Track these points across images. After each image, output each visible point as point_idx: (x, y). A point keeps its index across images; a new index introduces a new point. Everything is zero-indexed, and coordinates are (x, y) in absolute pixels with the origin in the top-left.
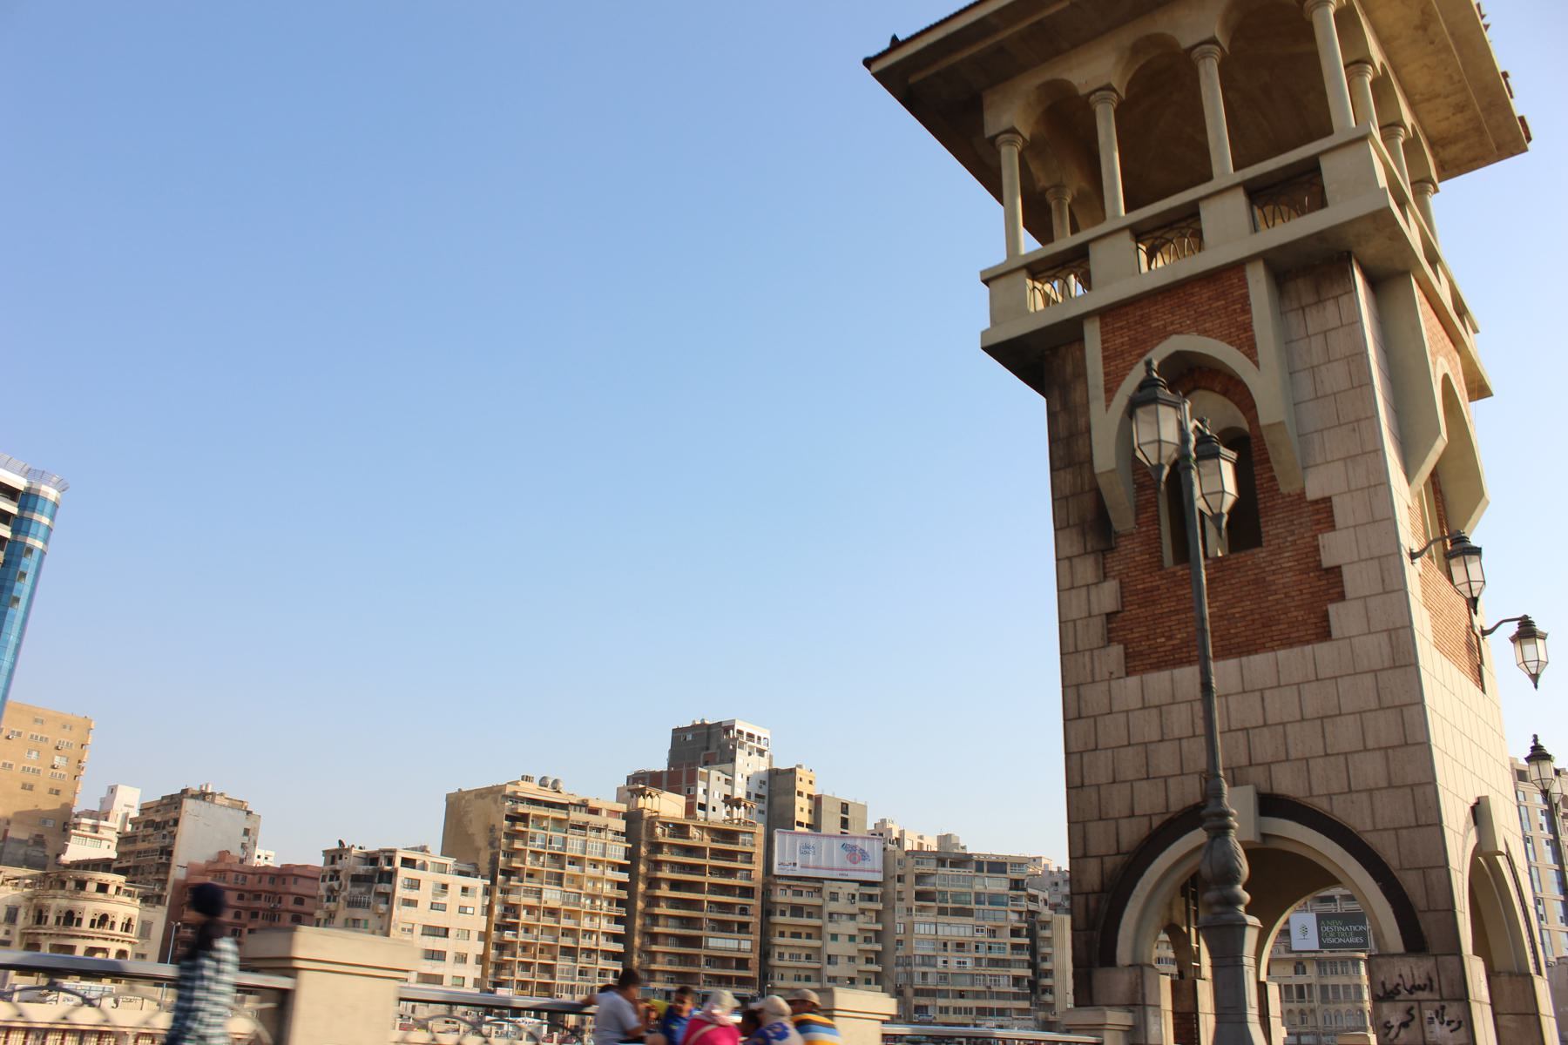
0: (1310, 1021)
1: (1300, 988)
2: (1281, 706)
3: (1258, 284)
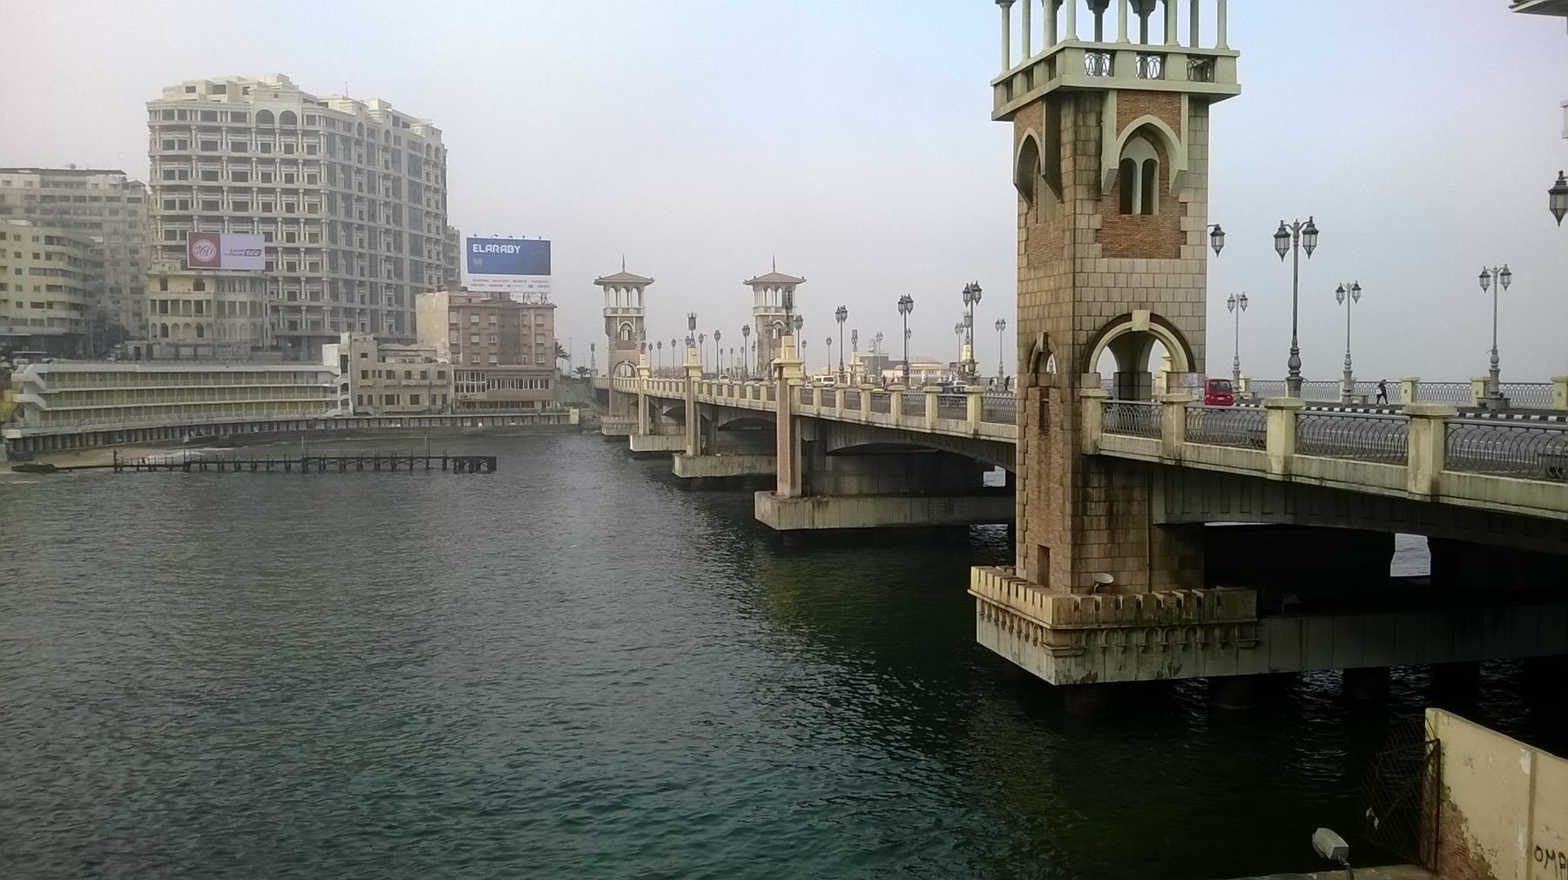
0: (207, 334)
1: (199, 304)
2: (1160, 281)
3: (1185, 102)
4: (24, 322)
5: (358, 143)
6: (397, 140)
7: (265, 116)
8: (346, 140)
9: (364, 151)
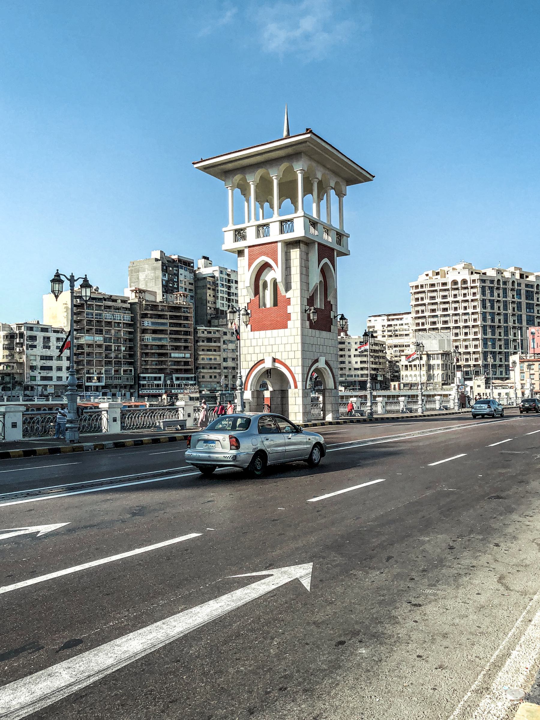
4: (352, 376)
5: (498, 288)
6: (519, 285)
7: (455, 282)
8: (491, 289)
9: (501, 292)
